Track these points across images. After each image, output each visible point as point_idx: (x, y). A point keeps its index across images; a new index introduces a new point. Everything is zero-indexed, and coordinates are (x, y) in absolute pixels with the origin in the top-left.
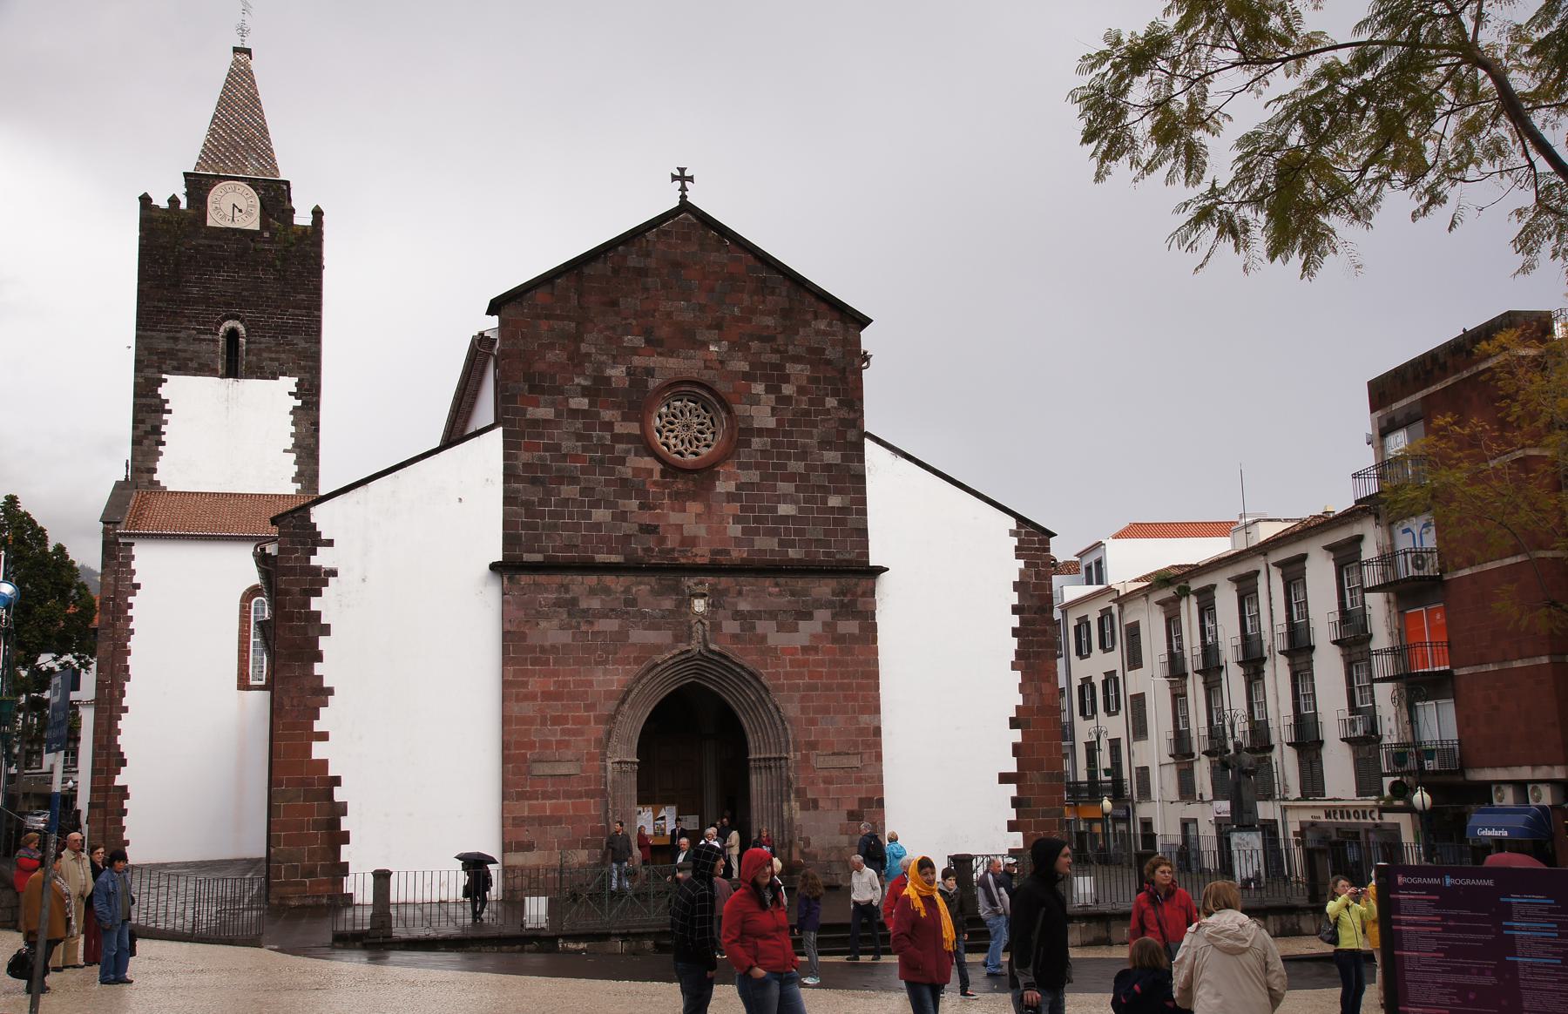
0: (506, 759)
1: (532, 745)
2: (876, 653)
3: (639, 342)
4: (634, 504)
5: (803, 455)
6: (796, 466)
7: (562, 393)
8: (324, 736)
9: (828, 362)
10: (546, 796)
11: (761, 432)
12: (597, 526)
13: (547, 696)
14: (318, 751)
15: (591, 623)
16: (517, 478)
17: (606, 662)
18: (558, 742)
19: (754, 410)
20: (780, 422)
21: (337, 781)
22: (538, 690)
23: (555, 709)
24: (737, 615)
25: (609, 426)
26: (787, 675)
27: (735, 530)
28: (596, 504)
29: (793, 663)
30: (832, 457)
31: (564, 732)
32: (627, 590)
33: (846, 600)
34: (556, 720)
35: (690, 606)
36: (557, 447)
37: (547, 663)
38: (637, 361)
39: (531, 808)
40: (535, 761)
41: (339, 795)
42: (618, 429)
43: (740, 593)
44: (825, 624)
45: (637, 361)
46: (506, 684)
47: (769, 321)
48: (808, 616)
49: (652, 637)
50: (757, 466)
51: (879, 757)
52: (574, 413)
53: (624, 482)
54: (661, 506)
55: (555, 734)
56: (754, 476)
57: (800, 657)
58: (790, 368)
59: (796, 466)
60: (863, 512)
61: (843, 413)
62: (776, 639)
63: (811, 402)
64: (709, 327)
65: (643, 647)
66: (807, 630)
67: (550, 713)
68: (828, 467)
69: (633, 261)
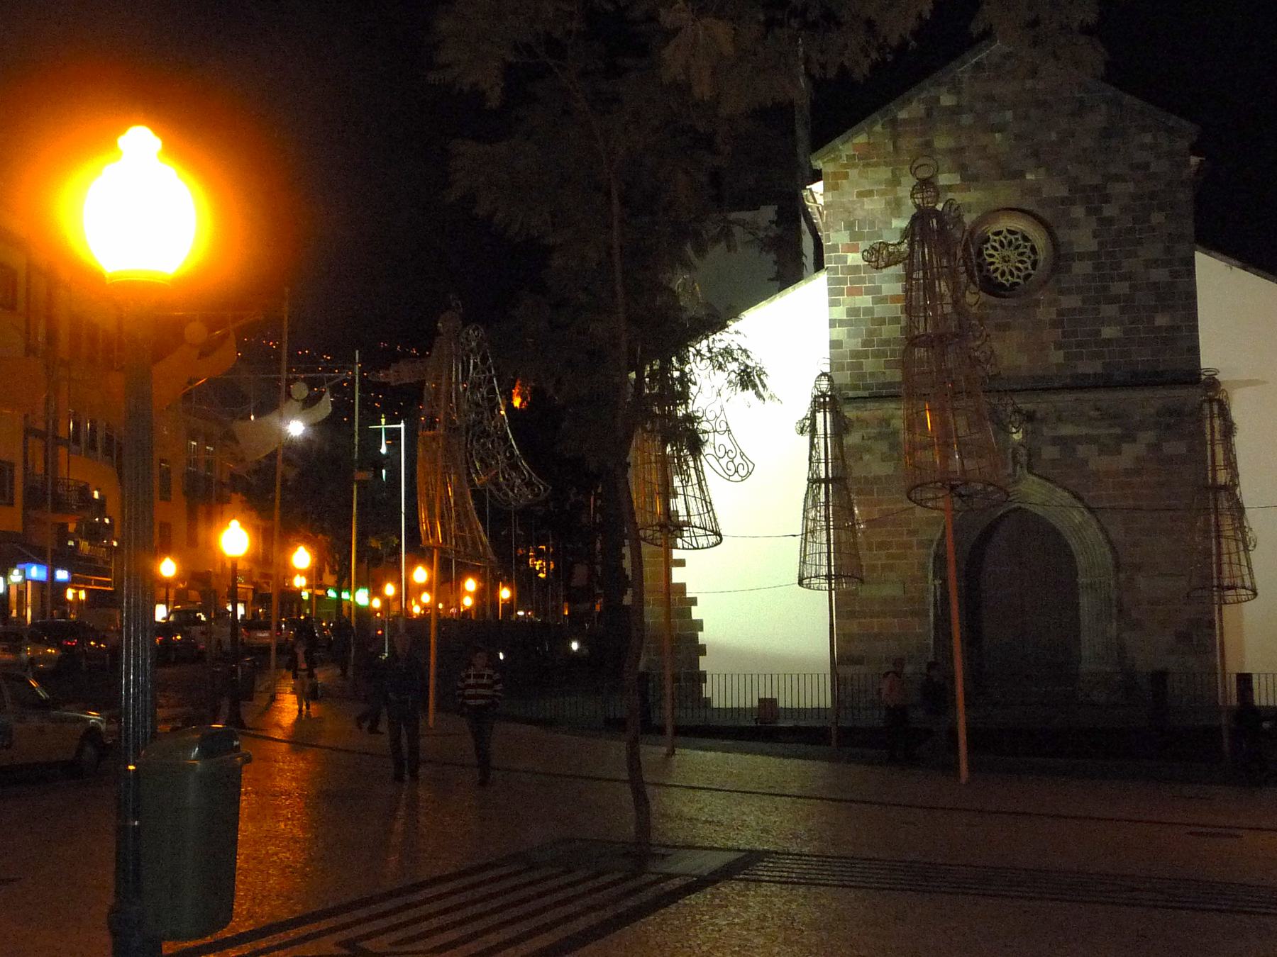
6: (1120, 288)
8: (681, 563)
11: (1081, 256)
14: (677, 575)
18: (884, 567)
21: (694, 601)
24: (1057, 441)
27: (1057, 357)
34: (881, 545)
41: (696, 613)
43: (1059, 419)
44: (1148, 445)
56: (1072, 301)
58: (1116, 188)
59: (1120, 288)
60: (1195, 328)
62: (1099, 463)
66: (1129, 454)
69: (947, 100)
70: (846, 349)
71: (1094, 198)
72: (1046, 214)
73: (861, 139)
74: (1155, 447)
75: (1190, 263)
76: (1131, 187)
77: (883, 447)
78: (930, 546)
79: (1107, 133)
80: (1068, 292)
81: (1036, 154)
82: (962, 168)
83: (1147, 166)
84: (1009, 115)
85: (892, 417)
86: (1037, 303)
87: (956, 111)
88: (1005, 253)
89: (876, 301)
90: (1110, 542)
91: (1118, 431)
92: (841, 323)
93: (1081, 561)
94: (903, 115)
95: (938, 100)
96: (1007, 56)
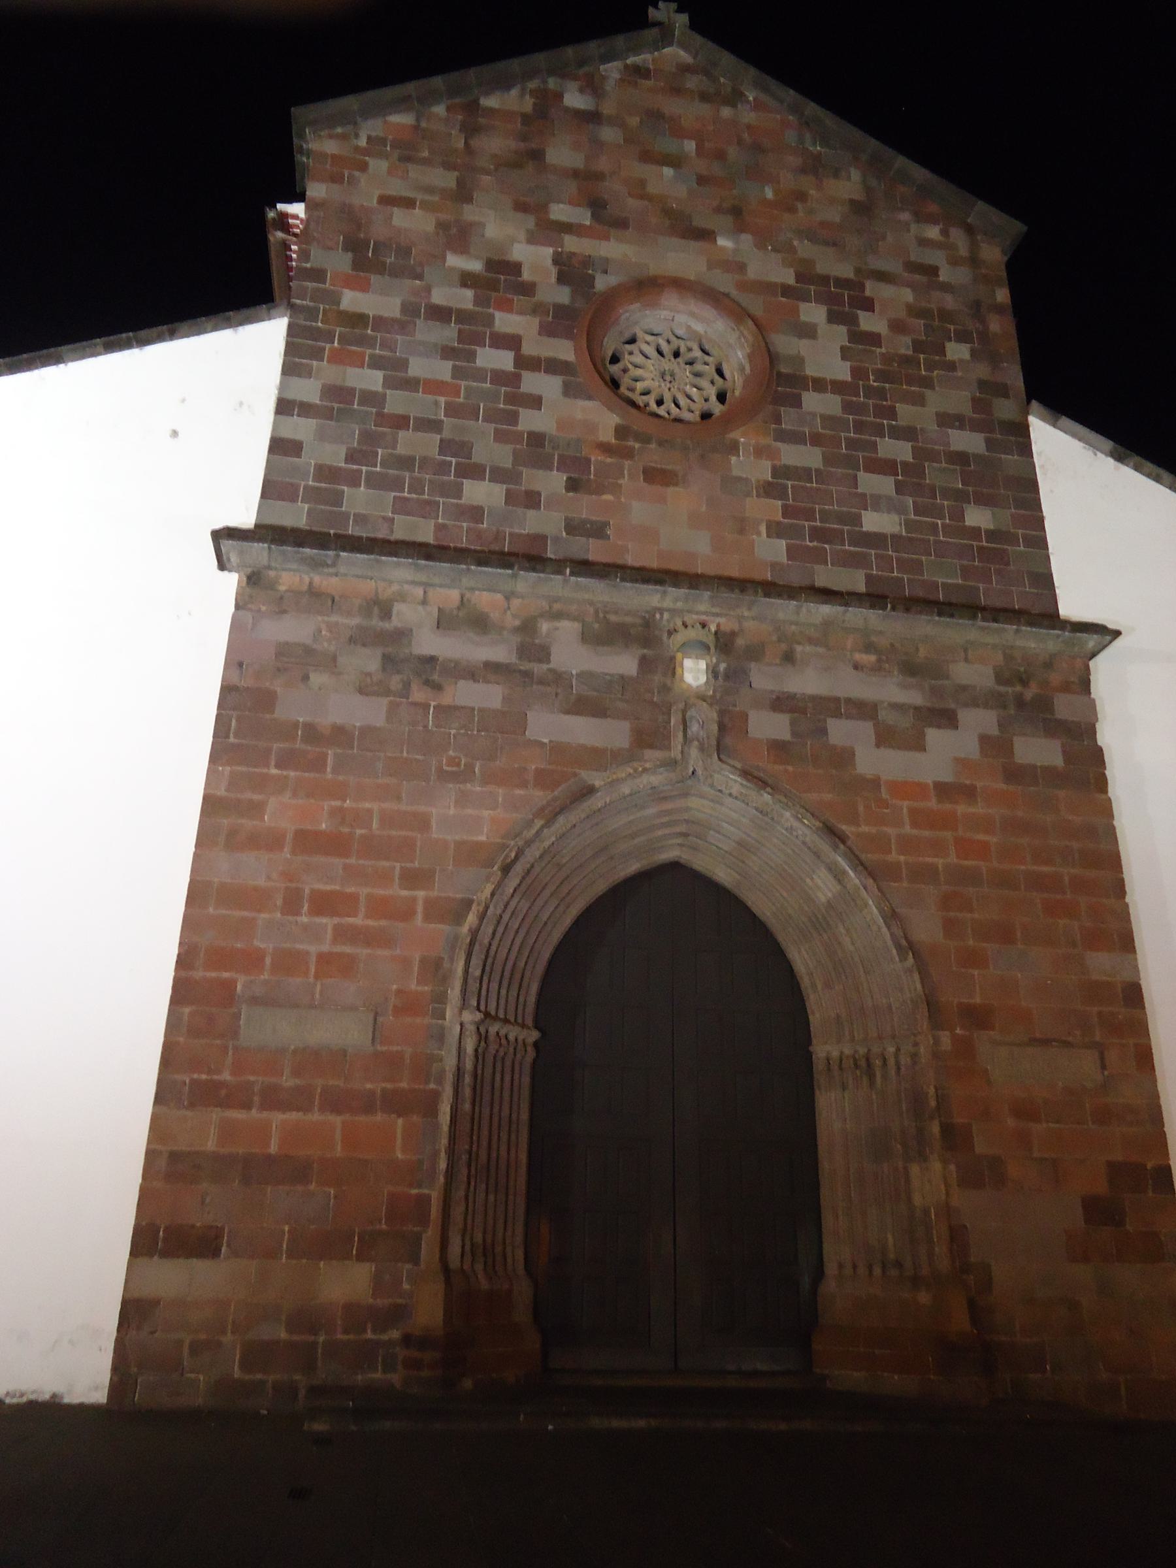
0: (182, 992)
1: (252, 961)
2: (1106, 811)
3: (584, 217)
4: (553, 482)
5: (908, 433)
7: (420, 277)
9: (946, 287)
10: (273, 1099)
11: (819, 385)
12: (476, 513)
13: (309, 842)
15: (438, 687)
16: (306, 409)
17: (463, 775)
18: (325, 960)
19: (802, 347)
20: (857, 372)
22: (288, 826)
23: (325, 875)
25: (512, 342)
26: (906, 844)
28: (474, 472)
29: (918, 818)
30: (969, 442)
31: (341, 934)
32: (527, 627)
33: (1029, 694)
34: (324, 904)
35: (671, 668)
36: (403, 364)
37: (318, 764)
38: (571, 243)
39: (228, 1132)
40: (254, 1001)
42: (528, 349)
43: (788, 658)
44: (984, 740)
45: (571, 243)
46: (210, 805)
47: (834, 215)
48: (947, 718)
49: (583, 731)
50: (816, 440)
51: (1145, 1058)
52: (441, 314)
53: (537, 439)
54: (616, 489)
55: (317, 936)
57: (932, 804)
60: (1040, 542)
61: (982, 371)
63: (918, 346)
64: (718, 210)
65: (558, 750)
66: (944, 753)
67: (312, 884)
68: (961, 458)
69: (575, 99)
70: (309, 459)
71: (846, 300)
72: (755, 304)
73: (402, 119)
74: (996, 746)
75: (1022, 431)
76: (907, 295)
77: (369, 661)
78: (458, 917)
79: (861, 209)
80: (795, 438)
81: (737, 212)
82: (597, 206)
83: (933, 271)
84: (690, 146)
85: (402, 597)
86: (734, 448)
87: (592, 118)
88: (668, 364)
89: (388, 383)
90: (908, 947)
91: (915, 698)
92: (306, 409)
93: (821, 1006)
94: (491, 102)
95: (559, 96)
96: (685, 69)
